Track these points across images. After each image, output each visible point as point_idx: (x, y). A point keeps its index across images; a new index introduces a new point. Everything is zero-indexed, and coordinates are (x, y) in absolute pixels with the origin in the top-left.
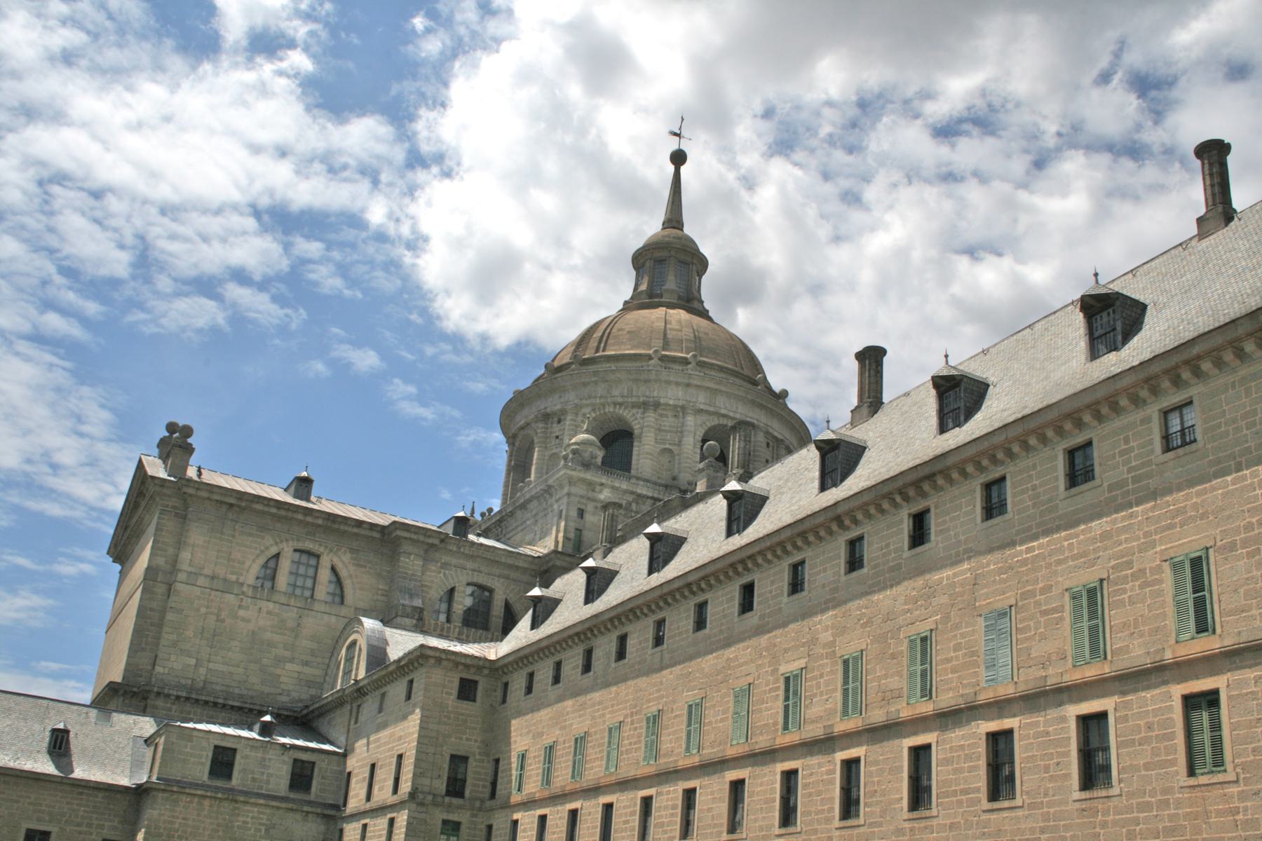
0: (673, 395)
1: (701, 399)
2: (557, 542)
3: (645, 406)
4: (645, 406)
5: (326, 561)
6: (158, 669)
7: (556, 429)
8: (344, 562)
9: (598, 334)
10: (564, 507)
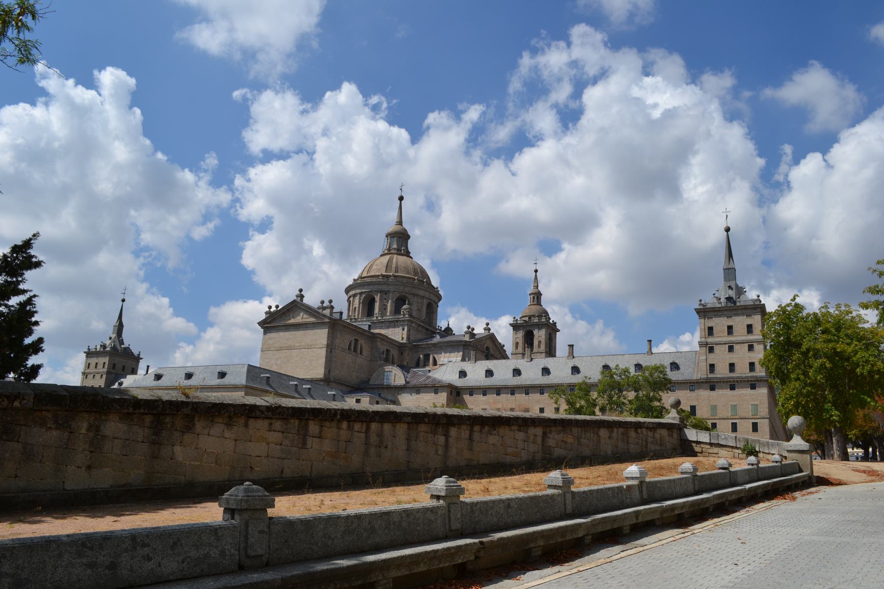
0: (421, 293)
1: (427, 295)
2: (403, 339)
3: (414, 295)
4: (414, 295)
5: (360, 342)
6: (332, 374)
7: (385, 296)
8: (361, 342)
9: (394, 266)
10: (406, 328)
